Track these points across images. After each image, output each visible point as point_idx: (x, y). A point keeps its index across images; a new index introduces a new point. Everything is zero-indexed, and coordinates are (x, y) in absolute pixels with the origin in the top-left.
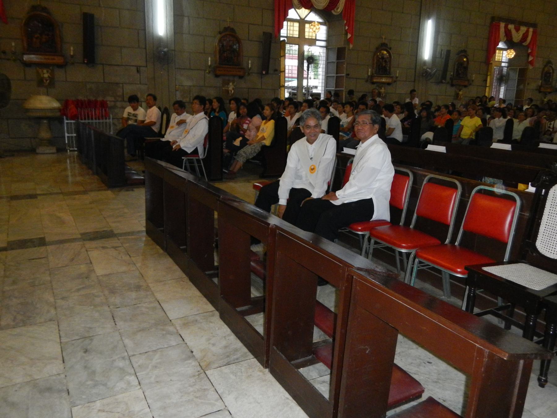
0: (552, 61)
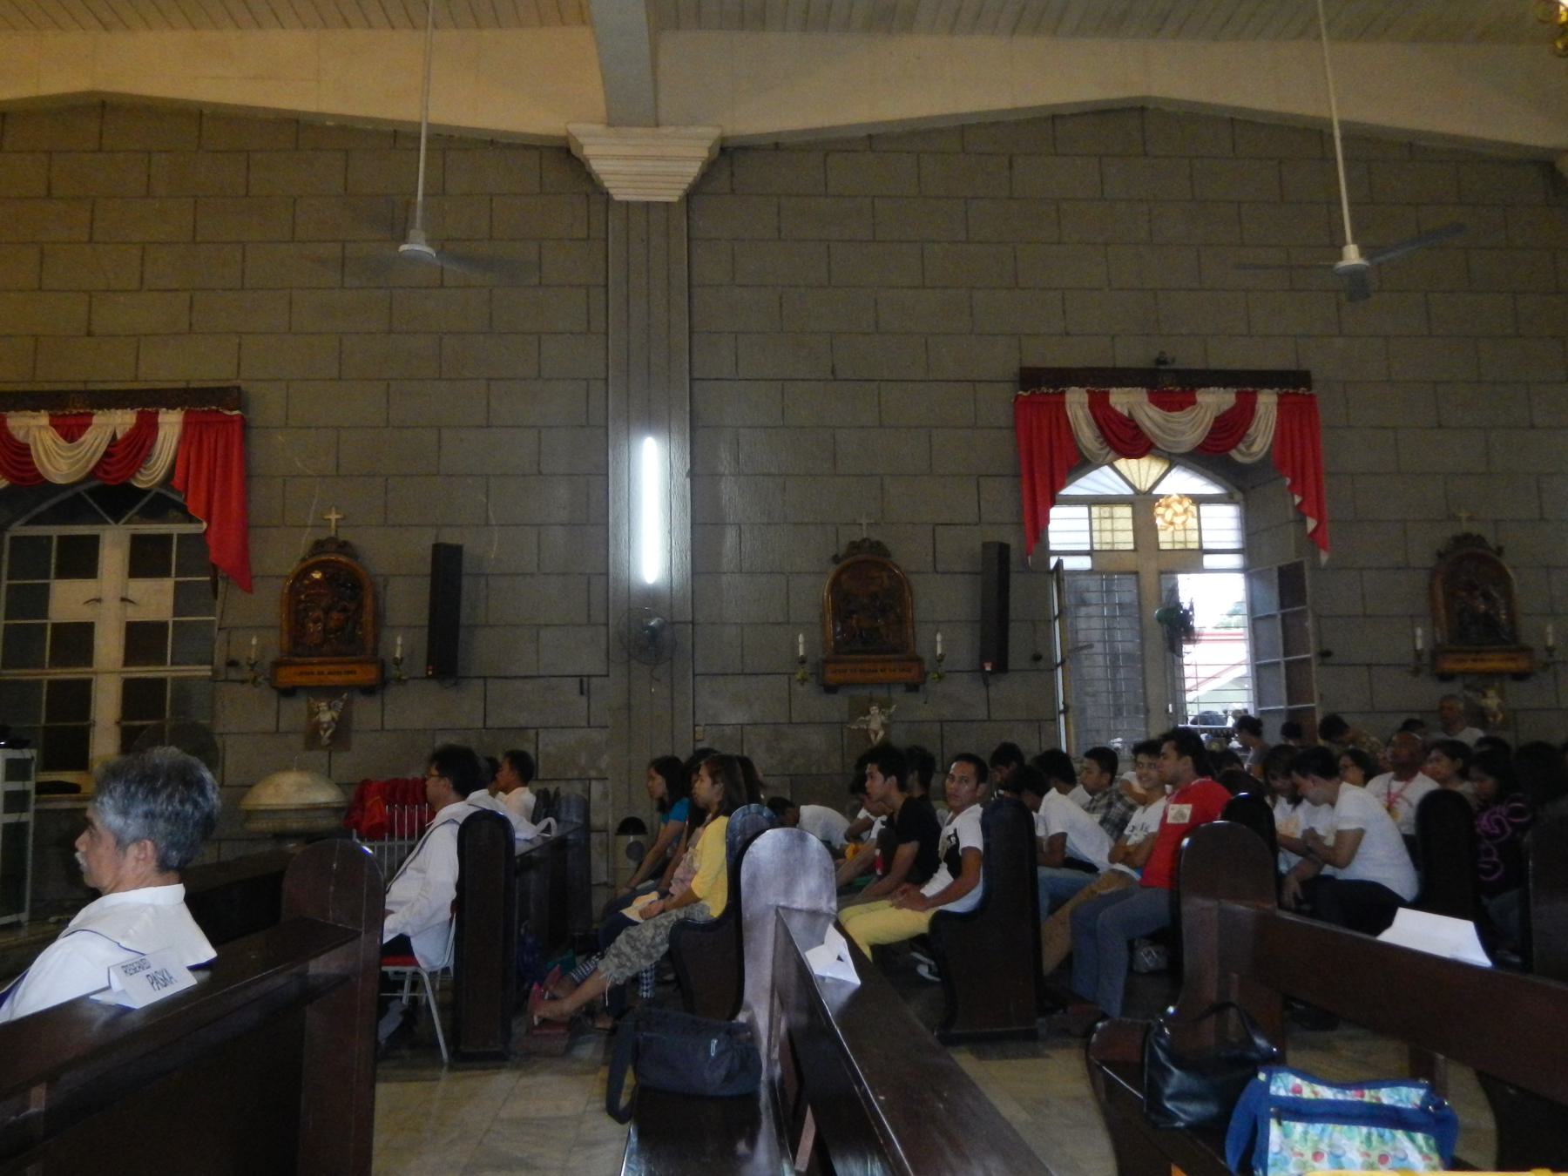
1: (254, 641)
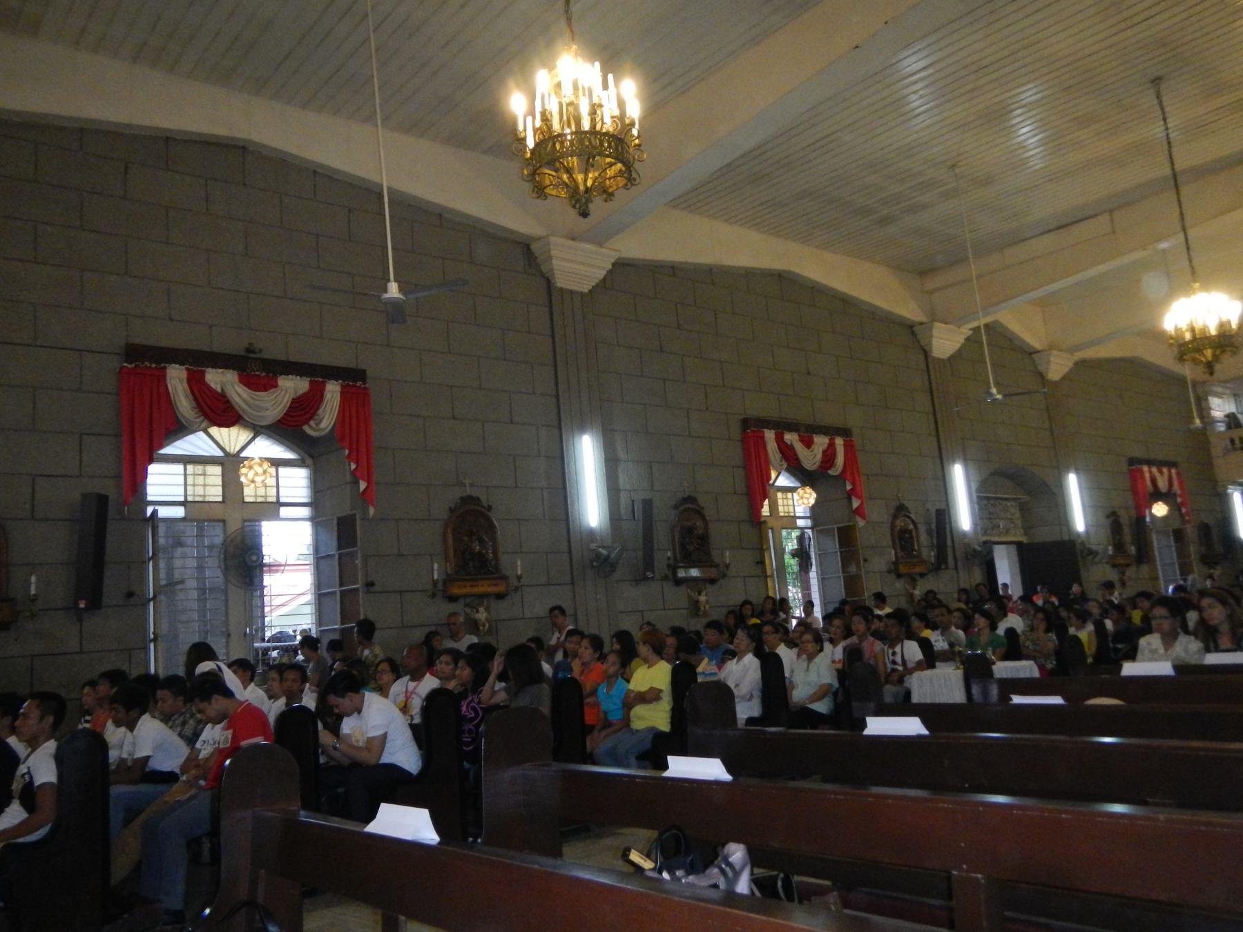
0: (906, 503)
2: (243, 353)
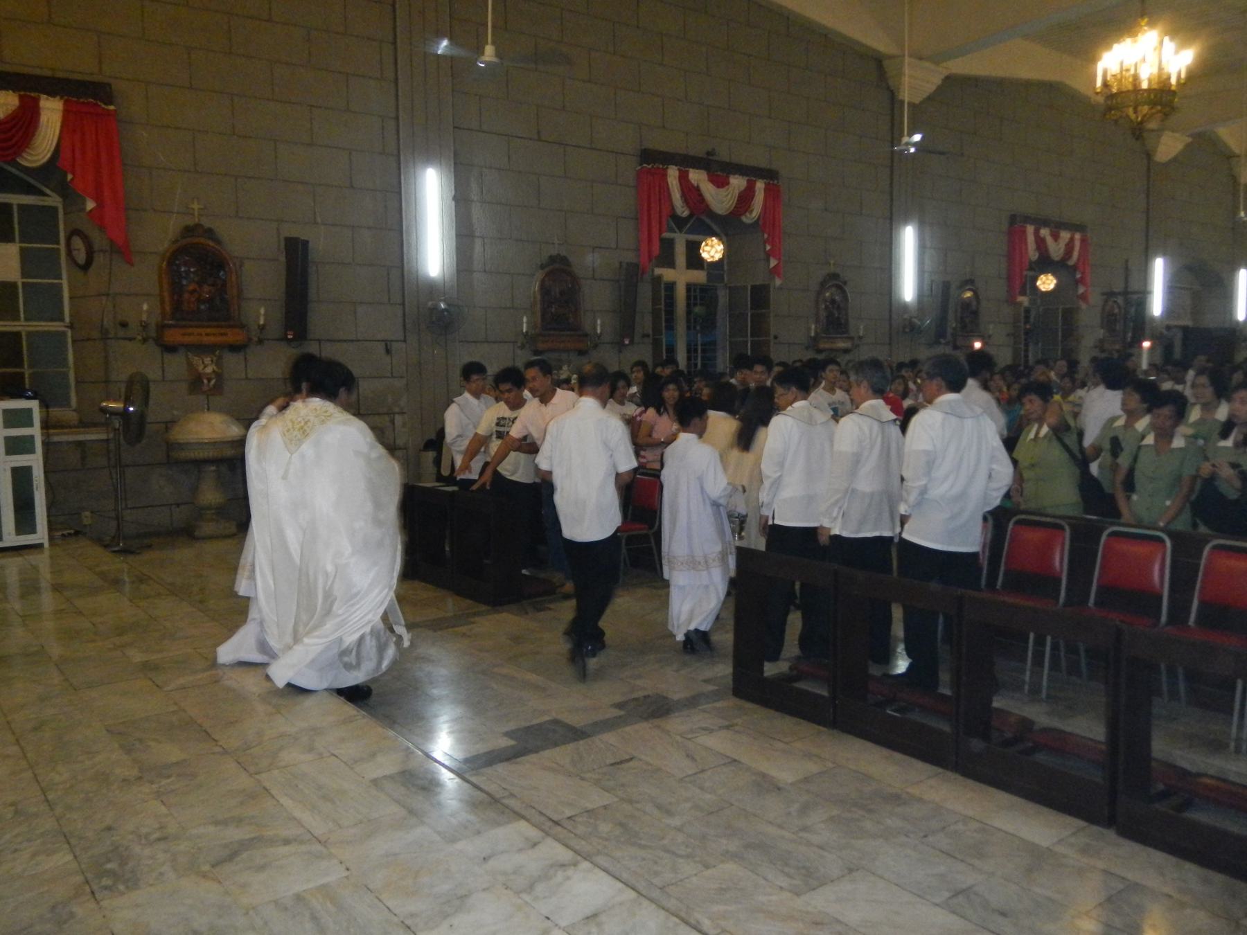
1: (145, 307)
2: (705, 156)
